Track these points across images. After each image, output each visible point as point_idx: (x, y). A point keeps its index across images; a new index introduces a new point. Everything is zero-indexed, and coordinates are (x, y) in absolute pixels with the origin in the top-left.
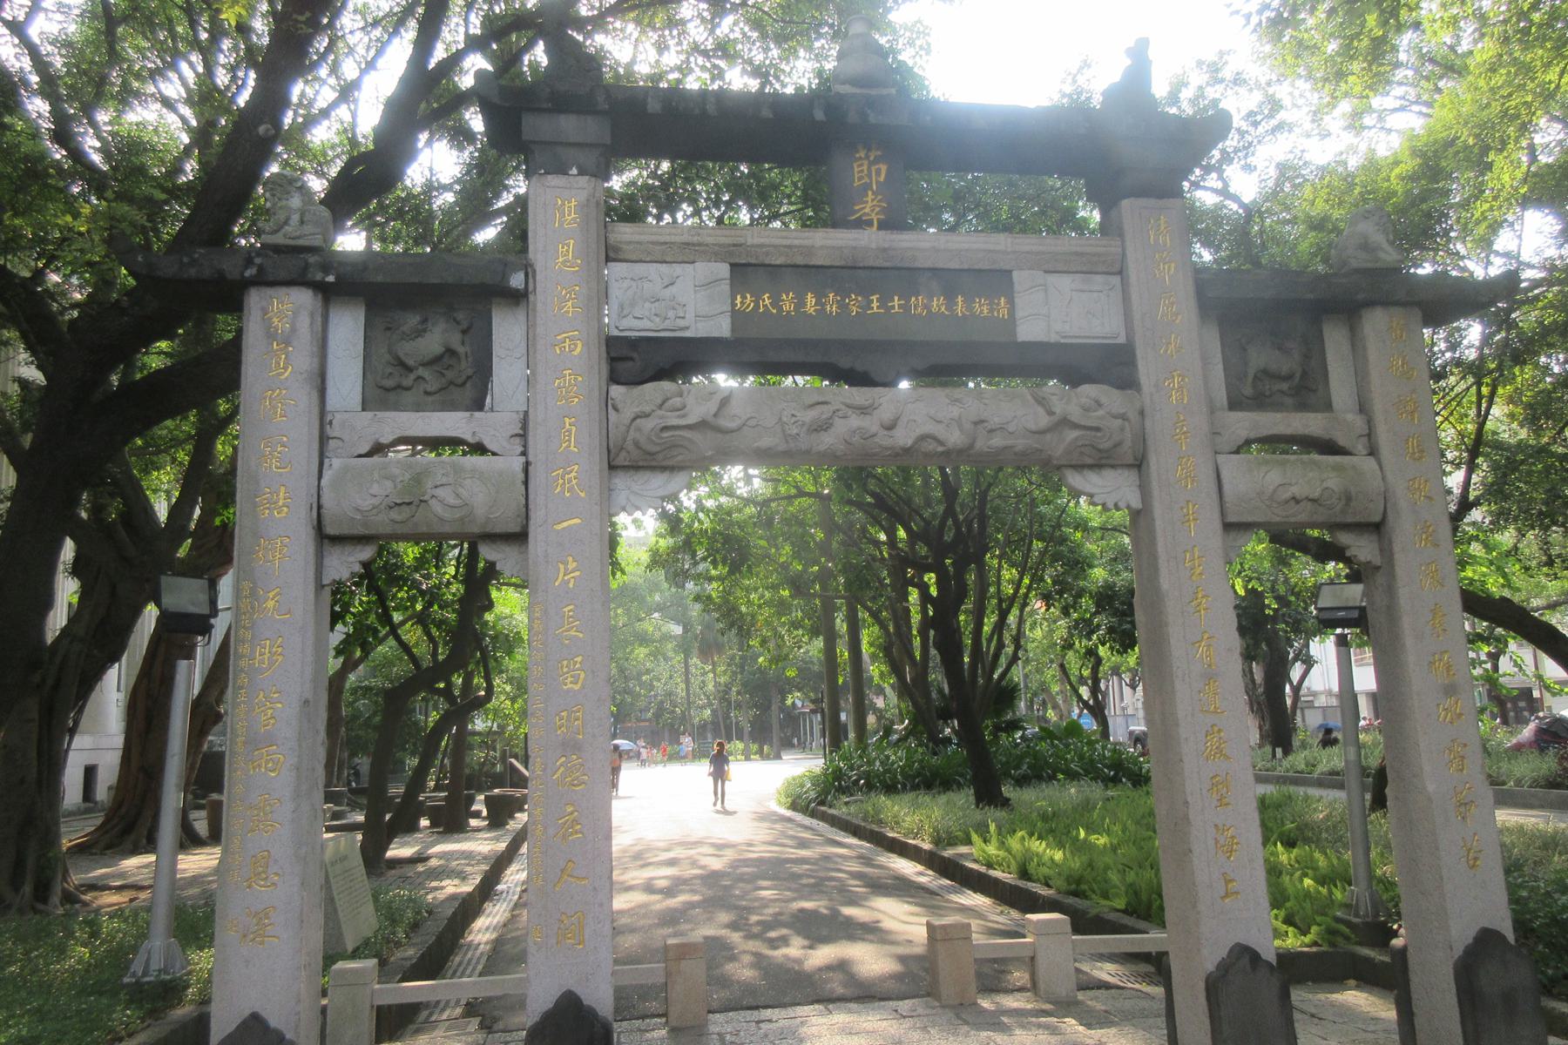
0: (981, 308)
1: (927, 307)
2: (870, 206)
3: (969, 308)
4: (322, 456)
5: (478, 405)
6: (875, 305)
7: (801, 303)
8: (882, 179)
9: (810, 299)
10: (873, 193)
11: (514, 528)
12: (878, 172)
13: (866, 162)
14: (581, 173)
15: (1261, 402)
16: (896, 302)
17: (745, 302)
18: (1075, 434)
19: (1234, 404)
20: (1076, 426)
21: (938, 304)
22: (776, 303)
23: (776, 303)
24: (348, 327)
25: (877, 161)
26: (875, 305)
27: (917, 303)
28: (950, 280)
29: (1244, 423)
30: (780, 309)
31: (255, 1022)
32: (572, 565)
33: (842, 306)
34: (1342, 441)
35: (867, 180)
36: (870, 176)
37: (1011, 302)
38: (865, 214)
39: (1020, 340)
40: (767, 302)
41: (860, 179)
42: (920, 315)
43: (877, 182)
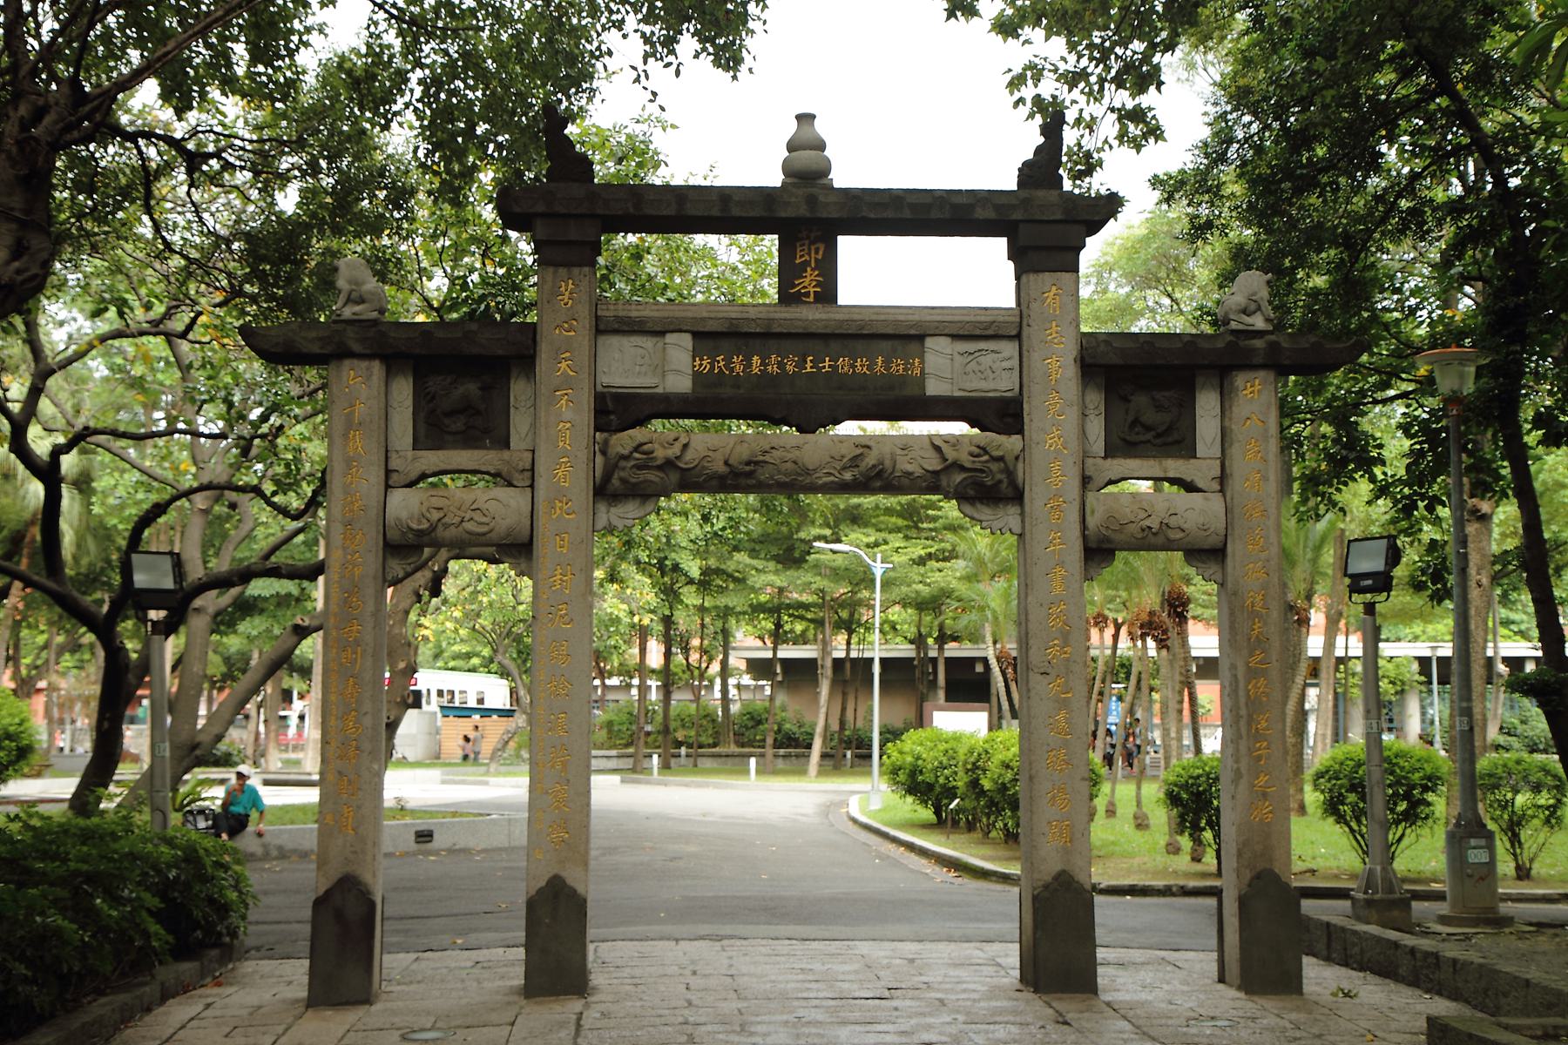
3: (888, 368)
4: (388, 487)
6: (809, 364)
8: (820, 257)
9: (756, 359)
10: (813, 270)
12: (817, 253)
13: (807, 242)
16: (827, 364)
18: (964, 475)
20: (963, 468)
22: (728, 361)
23: (728, 361)
24: (403, 391)
26: (809, 364)
30: (732, 370)
33: (781, 365)
35: (807, 257)
36: (809, 254)
37: (922, 362)
38: (805, 287)
39: (928, 393)
40: (722, 364)
41: (801, 256)
42: (846, 374)
43: (816, 260)
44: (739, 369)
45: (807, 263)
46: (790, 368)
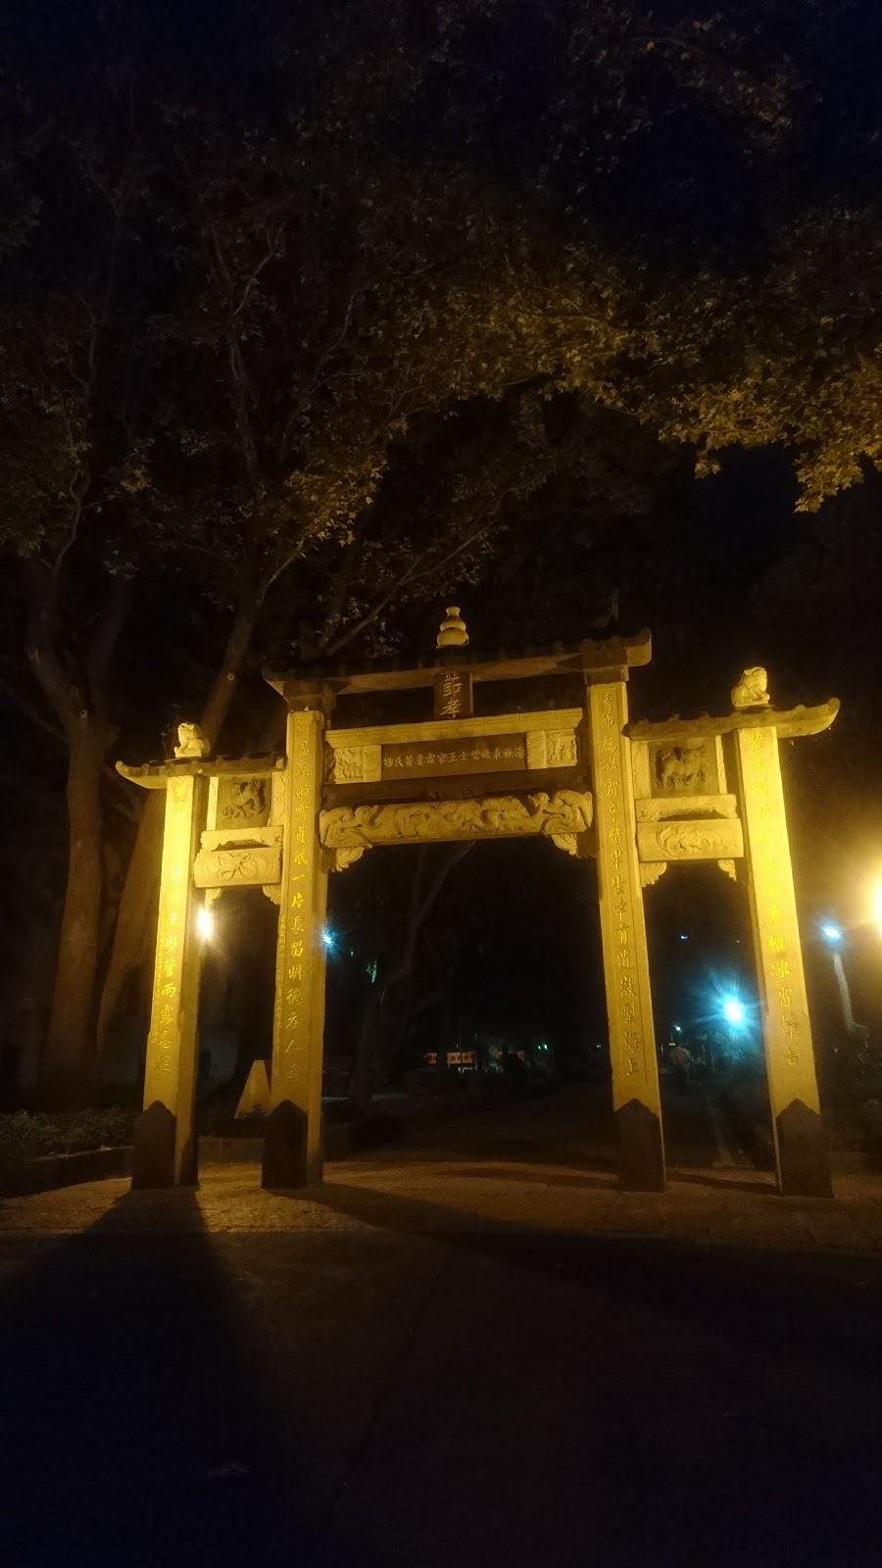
0: (508, 753)
1: (479, 756)
2: (452, 707)
5: (264, 824)
7: (416, 761)
11: (276, 880)
14: (310, 709)
15: (672, 793)
17: (389, 762)
19: (655, 794)
21: (486, 754)
22: (403, 759)
25: (456, 681)
27: (475, 754)
28: (492, 742)
29: (657, 807)
30: (405, 764)
31: (158, 1106)
32: (299, 896)
34: (719, 810)
44: (409, 763)
45: (451, 696)
46: (441, 761)
